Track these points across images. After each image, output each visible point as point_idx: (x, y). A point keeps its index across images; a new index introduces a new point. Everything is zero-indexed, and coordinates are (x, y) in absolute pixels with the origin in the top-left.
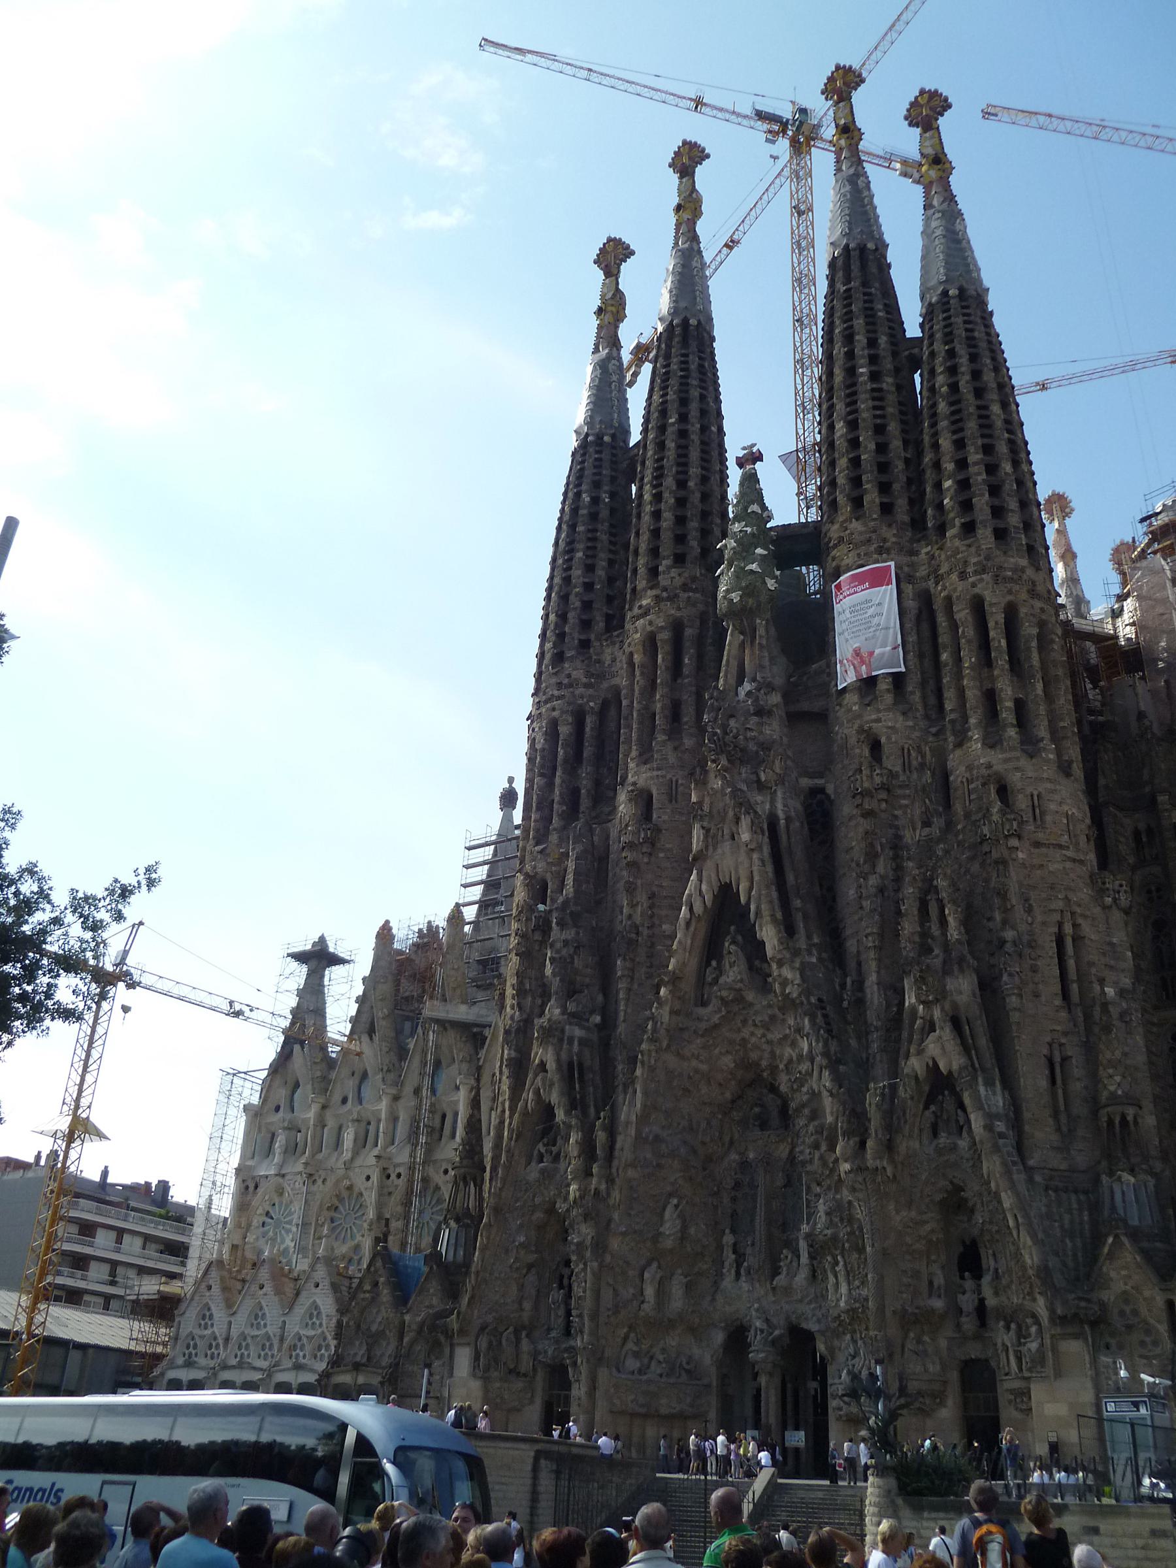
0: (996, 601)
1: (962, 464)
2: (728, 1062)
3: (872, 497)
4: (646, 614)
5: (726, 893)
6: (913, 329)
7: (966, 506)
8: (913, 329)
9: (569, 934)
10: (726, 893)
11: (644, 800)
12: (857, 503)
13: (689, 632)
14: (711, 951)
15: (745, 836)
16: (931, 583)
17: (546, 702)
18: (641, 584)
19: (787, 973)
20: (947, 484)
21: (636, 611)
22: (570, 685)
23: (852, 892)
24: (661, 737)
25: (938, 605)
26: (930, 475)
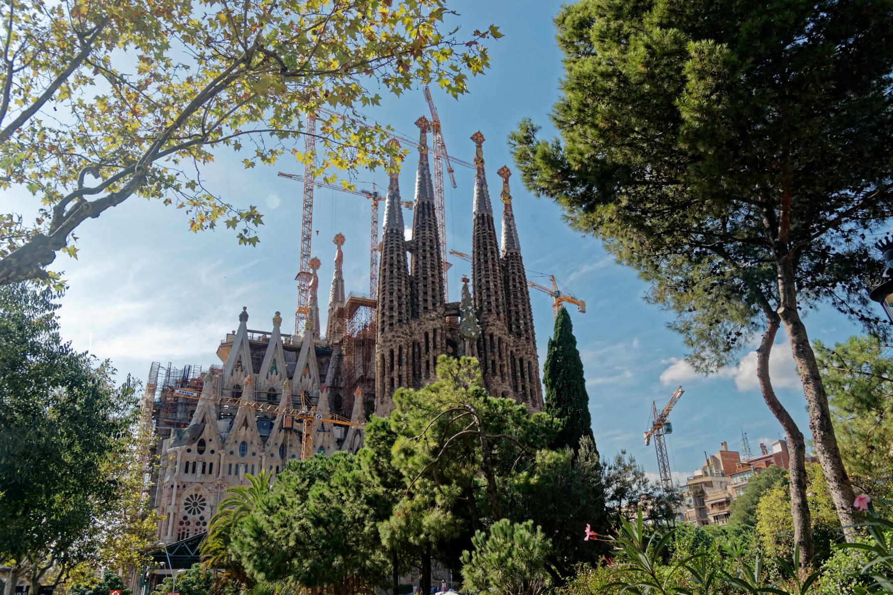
0: (533, 364)
1: (525, 317)
3: (502, 315)
4: (433, 320)
6: (502, 255)
7: (526, 331)
8: (502, 255)
12: (498, 314)
16: (514, 349)
17: (398, 337)
18: (430, 307)
21: (428, 316)
22: (406, 334)
25: (517, 358)
26: (513, 313)
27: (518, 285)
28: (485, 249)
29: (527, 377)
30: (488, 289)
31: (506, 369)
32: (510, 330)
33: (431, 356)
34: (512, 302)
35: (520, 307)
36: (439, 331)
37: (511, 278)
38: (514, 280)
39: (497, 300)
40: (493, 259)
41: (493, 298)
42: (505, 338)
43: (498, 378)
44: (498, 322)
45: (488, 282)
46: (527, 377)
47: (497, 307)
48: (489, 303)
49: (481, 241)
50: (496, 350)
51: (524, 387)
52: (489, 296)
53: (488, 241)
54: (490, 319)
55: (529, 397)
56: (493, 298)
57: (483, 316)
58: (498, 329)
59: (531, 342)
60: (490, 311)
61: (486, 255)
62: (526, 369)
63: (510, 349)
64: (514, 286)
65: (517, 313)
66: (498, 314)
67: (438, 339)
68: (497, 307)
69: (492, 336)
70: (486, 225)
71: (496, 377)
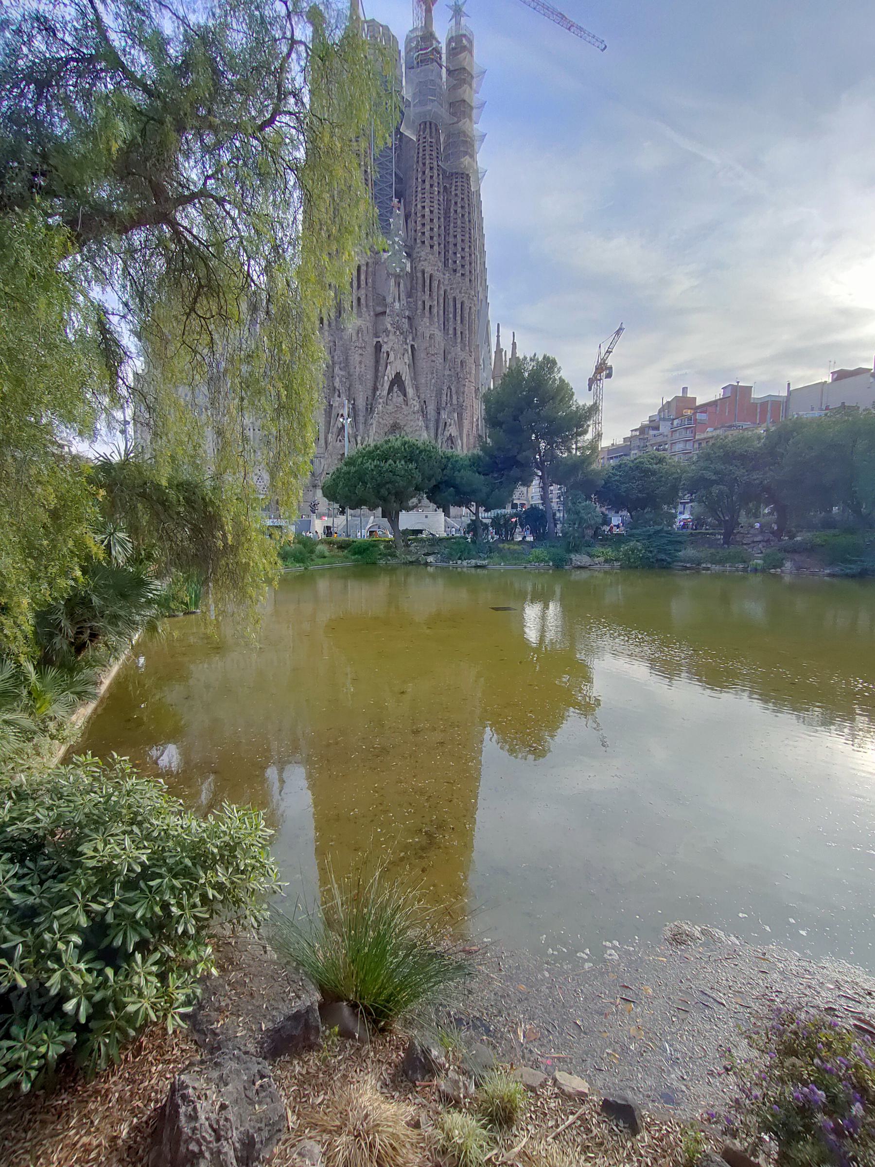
0: (467, 304)
1: (463, 249)
2: (391, 422)
3: (436, 247)
5: (398, 375)
7: (463, 266)
9: (342, 373)
10: (398, 375)
11: (359, 331)
12: (432, 247)
13: (370, 269)
14: (390, 390)
15: (406, 360)
19: (415, 402)
20: (458, 255)
23: (423, 381)
24: (365, 309)
26: (451, 246)
27: (459, 210)
28: (424, 164)
29: (458, 318)
30: (423, 216)
31: (435, 310)
32: (445, 265)
33: (354, 296)
34: (451, 231)
35: (459, 238)
36: (364, 268)
37: (453, 202)
38: (456, 203)
39: (432, 229)
40: (431, 177)
41: (428, 227)
42: (438, 275)
43: (426, 320)
44: (431, 256)
45: (424, 207)
46: (458, 318)
47: (432, 238)
48: (423, 233)
49: (421, 155)
50: (427, 288)
51: (455, 329)
52: (423, 225)
53: (427, 152)
54: (423, 254)
55: (459, 340)
56: (428, 227)
57: (417, 250)
58: (431, 263)
59: (467, 280)
60: (423, 242)
61: (424, 173)
62: (459, 311)
63: (443, 288)
64: (456, 211)
65: (455, 245)
66: (432, 247)
67: (363, 277)
68: (432, 238)
69: (423, 272)
70: (428, 130)
71: (425, 319)
